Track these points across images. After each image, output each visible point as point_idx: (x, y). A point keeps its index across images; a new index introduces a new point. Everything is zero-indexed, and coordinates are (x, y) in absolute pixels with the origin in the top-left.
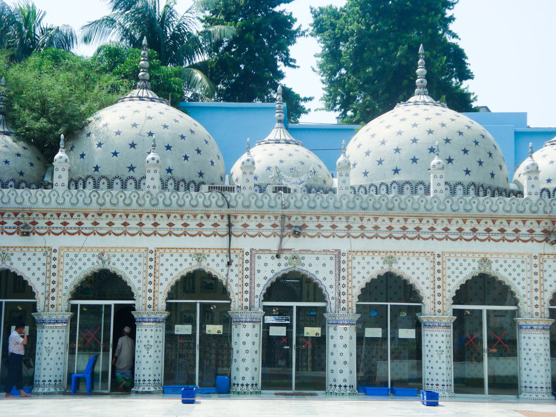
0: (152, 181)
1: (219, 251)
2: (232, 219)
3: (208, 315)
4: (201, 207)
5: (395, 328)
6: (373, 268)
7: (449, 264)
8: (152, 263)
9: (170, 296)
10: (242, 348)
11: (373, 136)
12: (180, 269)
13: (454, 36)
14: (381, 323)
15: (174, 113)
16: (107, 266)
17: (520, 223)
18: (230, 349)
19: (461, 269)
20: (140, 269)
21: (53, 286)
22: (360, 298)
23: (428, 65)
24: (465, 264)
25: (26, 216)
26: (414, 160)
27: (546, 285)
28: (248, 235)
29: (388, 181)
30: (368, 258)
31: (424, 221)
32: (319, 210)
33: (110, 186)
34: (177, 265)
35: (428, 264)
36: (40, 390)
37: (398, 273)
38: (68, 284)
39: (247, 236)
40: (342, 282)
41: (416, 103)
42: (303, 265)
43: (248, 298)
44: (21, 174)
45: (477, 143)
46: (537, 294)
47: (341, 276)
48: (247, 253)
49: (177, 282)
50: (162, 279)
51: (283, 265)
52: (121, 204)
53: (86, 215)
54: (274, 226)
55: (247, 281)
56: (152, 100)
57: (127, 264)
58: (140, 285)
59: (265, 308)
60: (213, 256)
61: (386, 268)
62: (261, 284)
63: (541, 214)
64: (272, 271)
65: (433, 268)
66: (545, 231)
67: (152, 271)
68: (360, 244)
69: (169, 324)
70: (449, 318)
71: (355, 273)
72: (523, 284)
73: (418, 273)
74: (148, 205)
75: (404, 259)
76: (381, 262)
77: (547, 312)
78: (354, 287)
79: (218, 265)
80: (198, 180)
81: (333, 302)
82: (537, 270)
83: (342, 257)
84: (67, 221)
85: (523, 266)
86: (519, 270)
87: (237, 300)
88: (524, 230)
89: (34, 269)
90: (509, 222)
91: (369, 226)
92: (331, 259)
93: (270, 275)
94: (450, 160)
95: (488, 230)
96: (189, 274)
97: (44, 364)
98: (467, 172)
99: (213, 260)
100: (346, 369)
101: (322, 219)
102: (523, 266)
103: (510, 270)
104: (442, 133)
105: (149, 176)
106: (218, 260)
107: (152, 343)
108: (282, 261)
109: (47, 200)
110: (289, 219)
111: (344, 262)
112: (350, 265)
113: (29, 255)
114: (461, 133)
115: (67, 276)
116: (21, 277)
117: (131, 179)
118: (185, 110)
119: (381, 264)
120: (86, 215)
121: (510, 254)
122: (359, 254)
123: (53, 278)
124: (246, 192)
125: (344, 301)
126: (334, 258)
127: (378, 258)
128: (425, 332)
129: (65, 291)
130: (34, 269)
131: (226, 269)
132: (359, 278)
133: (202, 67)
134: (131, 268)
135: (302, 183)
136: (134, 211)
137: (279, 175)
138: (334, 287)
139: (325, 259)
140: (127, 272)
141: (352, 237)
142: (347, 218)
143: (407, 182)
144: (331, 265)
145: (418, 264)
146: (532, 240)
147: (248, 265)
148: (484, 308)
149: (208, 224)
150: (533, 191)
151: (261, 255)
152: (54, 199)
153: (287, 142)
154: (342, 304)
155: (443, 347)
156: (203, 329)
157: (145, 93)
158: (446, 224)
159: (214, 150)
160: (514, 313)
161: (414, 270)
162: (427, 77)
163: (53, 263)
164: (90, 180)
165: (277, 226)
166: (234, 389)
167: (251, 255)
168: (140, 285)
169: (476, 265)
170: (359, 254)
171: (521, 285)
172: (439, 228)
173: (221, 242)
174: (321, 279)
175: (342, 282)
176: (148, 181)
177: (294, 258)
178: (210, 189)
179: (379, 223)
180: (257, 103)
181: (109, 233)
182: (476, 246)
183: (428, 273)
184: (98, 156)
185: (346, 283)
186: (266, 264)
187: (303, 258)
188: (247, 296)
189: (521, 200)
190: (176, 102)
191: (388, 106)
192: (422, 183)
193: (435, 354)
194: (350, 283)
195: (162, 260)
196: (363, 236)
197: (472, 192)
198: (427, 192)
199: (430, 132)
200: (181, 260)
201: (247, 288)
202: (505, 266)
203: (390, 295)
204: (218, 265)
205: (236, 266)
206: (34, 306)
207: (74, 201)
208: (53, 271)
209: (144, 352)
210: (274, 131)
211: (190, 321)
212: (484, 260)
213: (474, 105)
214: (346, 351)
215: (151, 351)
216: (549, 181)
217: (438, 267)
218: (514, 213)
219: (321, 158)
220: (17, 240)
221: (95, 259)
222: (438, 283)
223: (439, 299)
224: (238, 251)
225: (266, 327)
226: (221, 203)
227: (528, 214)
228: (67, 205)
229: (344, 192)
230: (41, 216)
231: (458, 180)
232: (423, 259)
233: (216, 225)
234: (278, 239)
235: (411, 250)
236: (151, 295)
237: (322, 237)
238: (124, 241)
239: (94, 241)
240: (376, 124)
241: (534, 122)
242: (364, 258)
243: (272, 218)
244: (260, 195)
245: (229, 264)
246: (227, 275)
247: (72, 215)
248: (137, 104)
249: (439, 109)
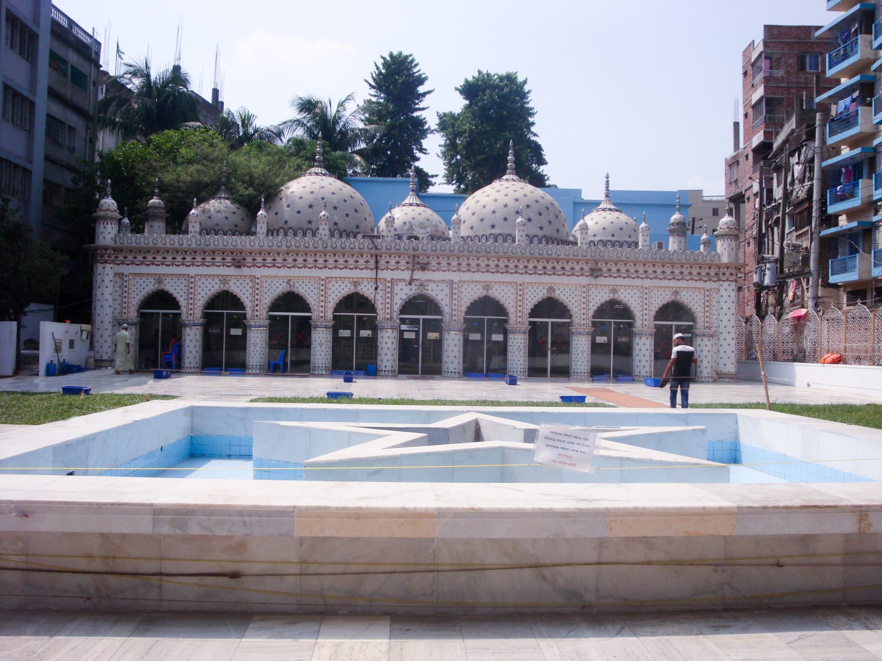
0: (324, 230)
2: (379, 258)
3: (363, 324)
4: (357, 249)
5: (490, 334)
7: (527, 291)
8: (323, 288)
9: (336, 310)
10: (385, 346)
11: (477, 202)
12: (343, 292)
13: (535, 135)
14: (479, 330)
15: (339, 184)
16: (293, 289)
17: (575, 263)
18: (377, 347)
19: (535, 294)
20: (315, 291)
21: (257, 302)
22: (467, 313)
23: (516, 154)
24: (538, 291)
26: (506, 219)
27: (591, 305)
29: (487, 233)
30: (472, 286)
31: (511, 261)
32: (439, 252)
33: (295, 235)
34: (340, 289)
35: (513, 290)
36: (250, 371)
37: (493, 296)
38: (267, 301)
40: (455, 302)
41: (507, 180)
44: (236, 226)
45: (548, 209)
46: (585, 311)
49: (340, 301)
50: (330, 299)
52: (302, 247)
53: (279, 254)
54: (408, 263)
55: (388, 300)
56: (324, 175)
57: (306, 288)
58: (315, 302)
59: (401, 319)
60: (365, 283)
61: (484, 293)
63: (589, 257)
65: (517, 293)
66: (591, 269)
67: (323, 293)
68: (467, 276)
69: (335, 330)
70: (526, 327)
71: (463, 296)
72: (576, 304)
73: (506, 297)
74: (320, 248)
75: (497, 287)
76: (481, 288)
77: (590, 323)
80: (356, 230)
81: (448, 315)
82: (585, 295)
84: (265, 258)
85: (576, 293)
86: (573, 295)
88: (577, 268)
89: (244, 290)
90: (568, 263)
93: (404, 297)
94: (529, 220)
95: (554, 268)
96: (348, 295)
97: (252, 355)
98: (541, 228)
100: (456, 361)
101: (441, 258)
102: (576, 293)
103: (567, 295)
104: (525, 201)
105: (321, 228)
106: (369, 286)
107: (323, 341)
108: (413, 287)
109: (252, 244)
113: (241, 281)
114: (537, 202)
115: (266, 296)
116: (236, 296)
117: (309, 229)
118: (347, 182)
120: (279, 254)
121: (568, 285)
123: (257, 297)
124: (388, 239)
127: (479, 286)
128: (511, 336)
129: (265, 306)
130: (244, 290)
131: (374, 292)
132: (465, 299)
133: (360, 152)
134: (309, 291)
136: (311, 251)
137: (411, 228)
139: (443, 286)
140: (306, 294)
142: (458, 258)
143: (500, 234)
144: (447, 290)
145: (506, 290)
146: (582, 275)
147: (389, 290)
148: (550, 320)
149: (362, 261)
150: (584, 242)
152: (257, 243)
153: (418, 205)
155: (522, 347)
156: (358, 333)
157: (319, 170)
159: (367, 209)
160: (569, 324)
161: (504, 295)
162: (515, 162)
163: (257, 286)
164: (282, 230)
166: (379, 373)
168: (315, 302)
169: (545, 291)
172: (521, 266)
173: (370, 274)
176: (321, 231)
178: (364, 237)
179: (480, 262)
180: (399, 178)
181: (294, 267)
182: (545, 279)
183: (513, 297)
184: (287, 213)
189: (576, 248)
190: (341, 176)
191: (489, 181)
192: (510, 235)
193: (516, 351)
195: (330, 286)
196: (469, 271)
197: (544, 242)
198: (514, 241)
199: (517, 200)
200: (343, 286)
201: (389, 306)
202: (564, 292)
203: (487, 312)
206: (244, 316)
207: (270, 244)
208: (257, 292)
209: (318, 348)
210: (409, 197)
211: (350, 327)
212: (551, 288)
213: (547, 183)
214: (456, 349)
215: (323, 348)
216: (595, 236)
217: (521, 293)
218: (571, 257)
219: (440, 216)
220: (232, 271)
221: (284, 285)
222: (520, 303)
223: (520, 314)
225: (402, 332)
226: (371, 246)
227: (580, 257)
228: (266, 247)
229: (457, 240)
231: (535, 233)
232: (509, 287)
233: (367, 262)
234: (410, 272)
235: (502, 280)
236: (323, 309)
238: (305, 272)
239: (284, 272)
240: (479, 193)
241: (586, 196)
244: (398, 241)
245: (376, 289)
247: (269, 254)
248: (313, 178)
249: (522, 184)
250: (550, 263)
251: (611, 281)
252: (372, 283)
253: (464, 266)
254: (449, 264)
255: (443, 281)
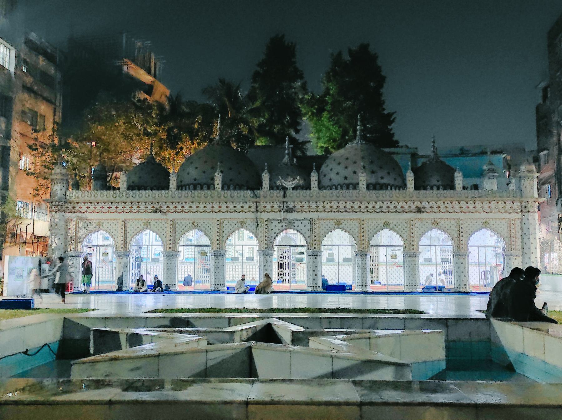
25: (157, 204)
35: (358, 225)
54: (280, 207)
75: (345, 222)
76: (334, 224)
91: (328, 206)
149: (246, 206)
158: (367, 204)
171: (405, 235)
173: (252, 216)
177: (290, 222)
196: (324, 211)
230: (164, 204)
250: (385, 203)
251: (432, 216)
253: (321, 209)
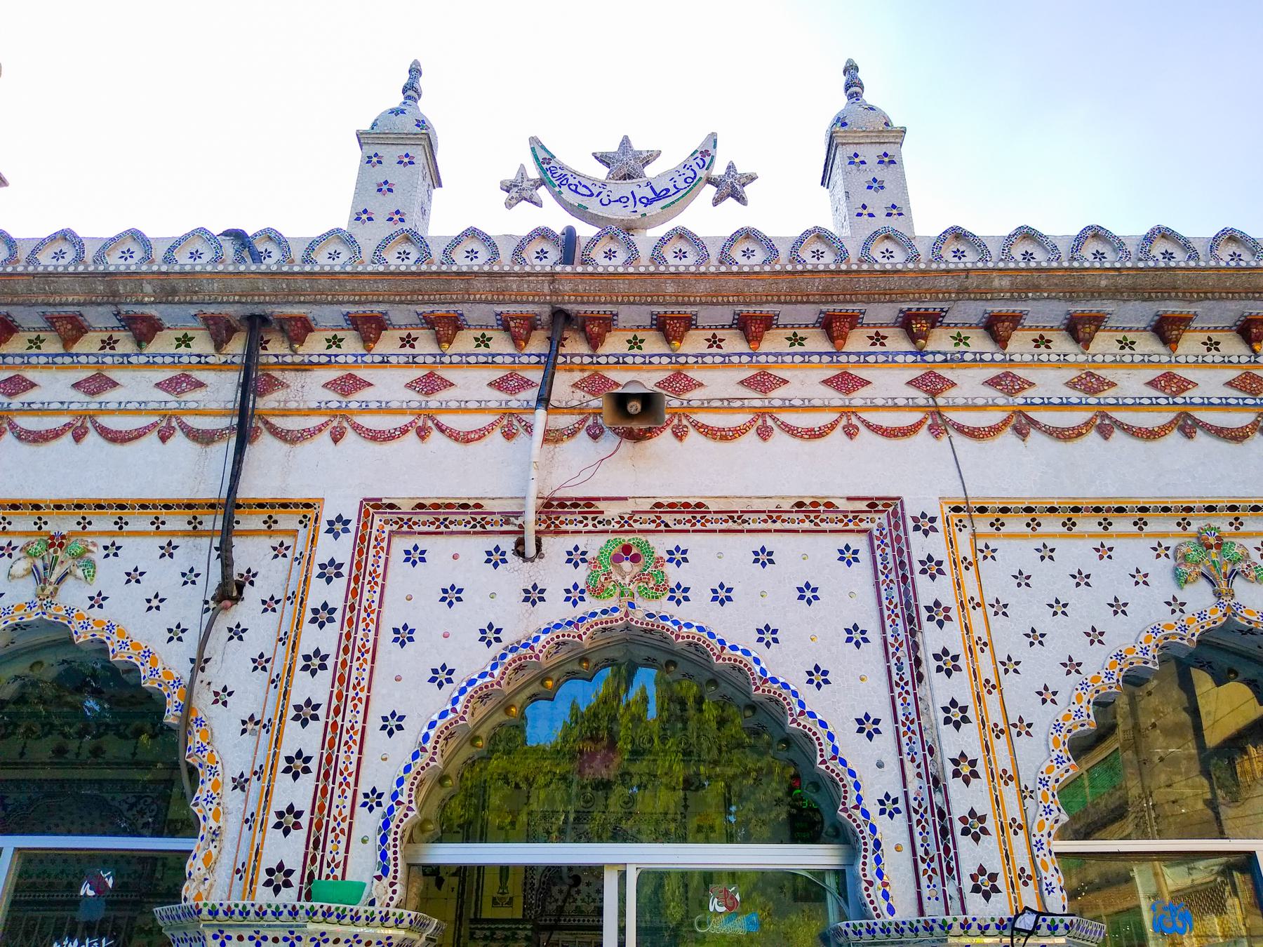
1: (176, 522)
6: (1118, 607)
28: (357, 428)
30: (1076, 552)
39: (350, 435)
42: (680, 594)
43: (304, 804)
47: (926, 654)
48: (337, 526)
51: (555, 595)
55: (316, 688)
60: (140, 550)
62: (411, 704)
64: (490, 634)
68: (1013, 469)
71: (1008, 636)
76: (1160, 571)
78: (1024, 727)
79: (155, 603)
81: (892, 831)
83: (916, 538)
87: (232, 826)
92: (848, 556)
93: (472, 660)
99: (134, 576)
108: (554, 572)
110: (595, 342)
111: (932, 567)
112: (971, 589)
119: (1162, 584)
122: (1015, 524)
125: (975, 826)
126: (864, 555)
127: (1133, 551)
135: (658, 197)
138: (887, 726)
141: (960, 429)
144: (853, 593)
151: (423, 542)
154: (964, 843)
165: (527, 384)
167: (362, 539)
170: (1015, 524)
174: (798, 681)
175: (940, 689)
185: (965, 698)
186: (451, 595)
187: (678, 557)
188: (297, 793)
194: (992, 701)
204: (155, 603)
205: (269, 605)
224: (288, 521)
237: (779, 436)
242: (1047, 554)
243: (501, 344)
245: (230, 591)
246: (200, 663)
252: (198, 553)
254: (845, 382)
255: (812, 513)
